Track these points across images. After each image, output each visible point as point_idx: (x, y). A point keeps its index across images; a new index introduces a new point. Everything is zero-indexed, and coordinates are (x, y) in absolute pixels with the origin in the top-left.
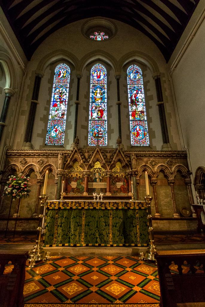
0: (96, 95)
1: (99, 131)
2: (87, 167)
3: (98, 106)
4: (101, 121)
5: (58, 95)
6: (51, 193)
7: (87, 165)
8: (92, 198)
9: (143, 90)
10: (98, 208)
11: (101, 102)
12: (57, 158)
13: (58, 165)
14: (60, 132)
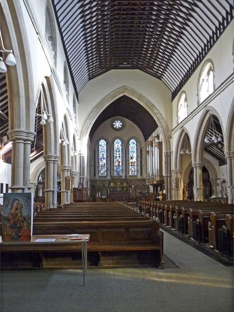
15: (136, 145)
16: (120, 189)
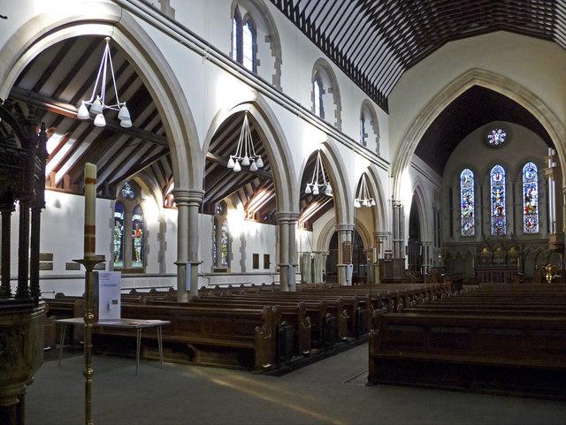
15: (538, 173)
16: (503, 261)
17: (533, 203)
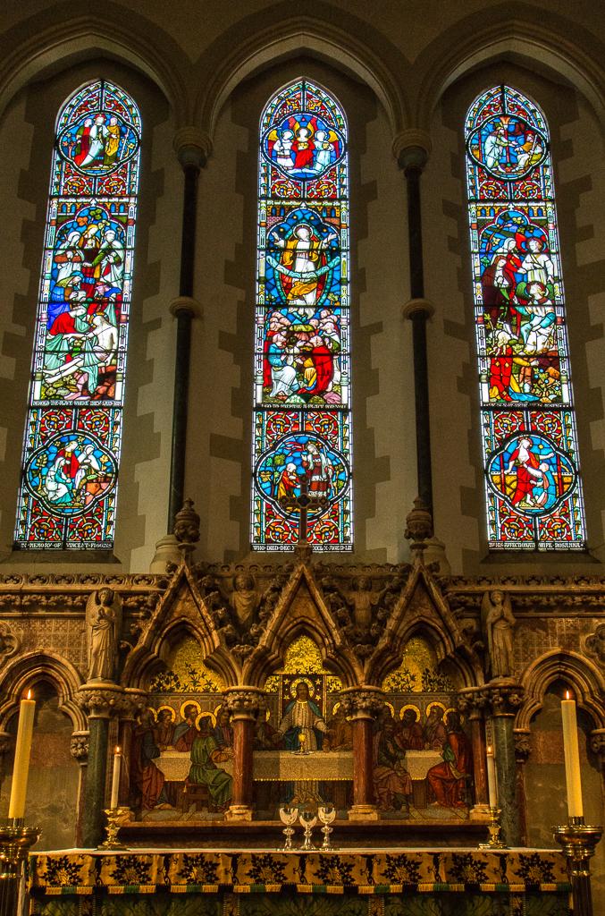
0: (288, 262)
1: (311, 466)
2: (247, 666)
3: (303, 328)
4: (319, 410)
5: (77, 267)
6: (53, 810)
7: (243, 657)
8: (275, 835)
9: (553, 236)
10: (308, 888)
11: (317, 307)
12: (83, 618)
13: (86, 660)
14: (90, 478)
17: (536, 341)
